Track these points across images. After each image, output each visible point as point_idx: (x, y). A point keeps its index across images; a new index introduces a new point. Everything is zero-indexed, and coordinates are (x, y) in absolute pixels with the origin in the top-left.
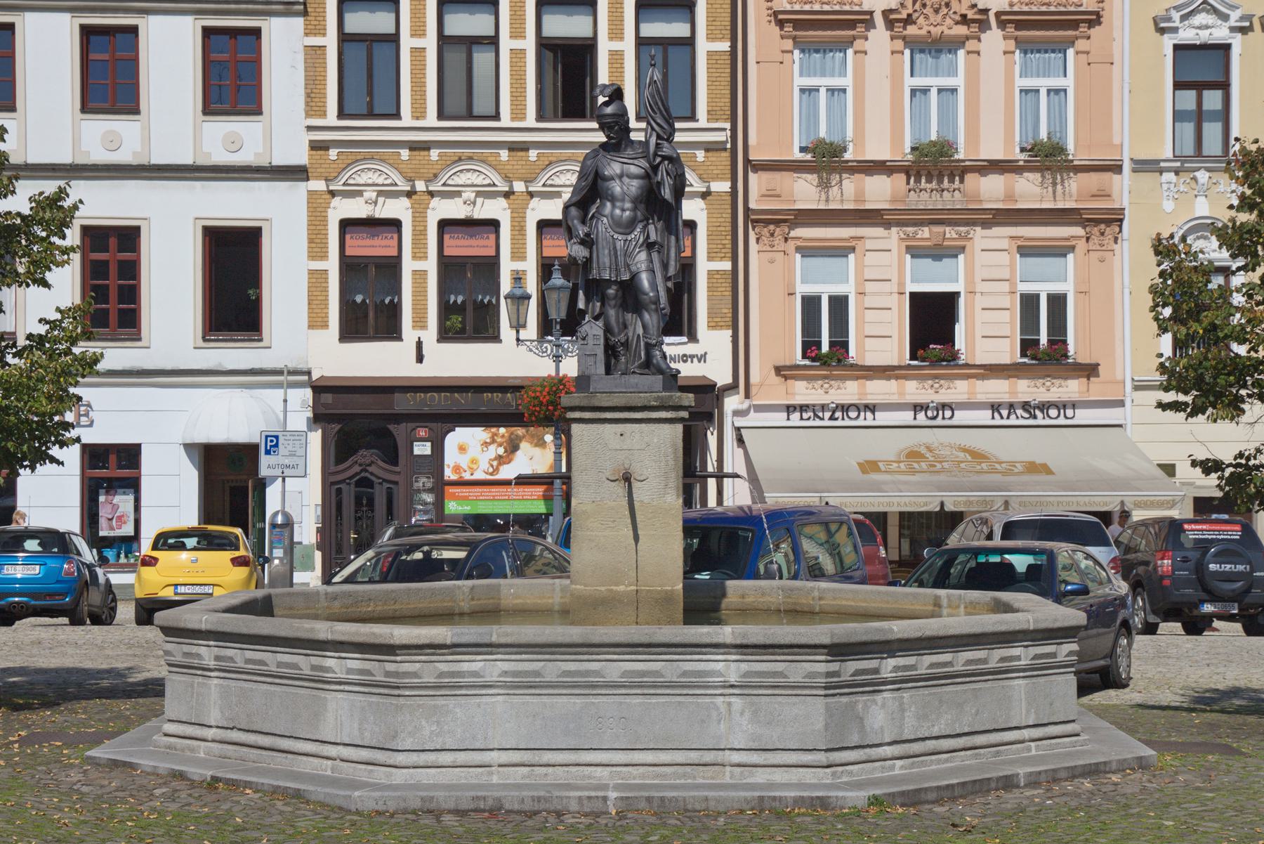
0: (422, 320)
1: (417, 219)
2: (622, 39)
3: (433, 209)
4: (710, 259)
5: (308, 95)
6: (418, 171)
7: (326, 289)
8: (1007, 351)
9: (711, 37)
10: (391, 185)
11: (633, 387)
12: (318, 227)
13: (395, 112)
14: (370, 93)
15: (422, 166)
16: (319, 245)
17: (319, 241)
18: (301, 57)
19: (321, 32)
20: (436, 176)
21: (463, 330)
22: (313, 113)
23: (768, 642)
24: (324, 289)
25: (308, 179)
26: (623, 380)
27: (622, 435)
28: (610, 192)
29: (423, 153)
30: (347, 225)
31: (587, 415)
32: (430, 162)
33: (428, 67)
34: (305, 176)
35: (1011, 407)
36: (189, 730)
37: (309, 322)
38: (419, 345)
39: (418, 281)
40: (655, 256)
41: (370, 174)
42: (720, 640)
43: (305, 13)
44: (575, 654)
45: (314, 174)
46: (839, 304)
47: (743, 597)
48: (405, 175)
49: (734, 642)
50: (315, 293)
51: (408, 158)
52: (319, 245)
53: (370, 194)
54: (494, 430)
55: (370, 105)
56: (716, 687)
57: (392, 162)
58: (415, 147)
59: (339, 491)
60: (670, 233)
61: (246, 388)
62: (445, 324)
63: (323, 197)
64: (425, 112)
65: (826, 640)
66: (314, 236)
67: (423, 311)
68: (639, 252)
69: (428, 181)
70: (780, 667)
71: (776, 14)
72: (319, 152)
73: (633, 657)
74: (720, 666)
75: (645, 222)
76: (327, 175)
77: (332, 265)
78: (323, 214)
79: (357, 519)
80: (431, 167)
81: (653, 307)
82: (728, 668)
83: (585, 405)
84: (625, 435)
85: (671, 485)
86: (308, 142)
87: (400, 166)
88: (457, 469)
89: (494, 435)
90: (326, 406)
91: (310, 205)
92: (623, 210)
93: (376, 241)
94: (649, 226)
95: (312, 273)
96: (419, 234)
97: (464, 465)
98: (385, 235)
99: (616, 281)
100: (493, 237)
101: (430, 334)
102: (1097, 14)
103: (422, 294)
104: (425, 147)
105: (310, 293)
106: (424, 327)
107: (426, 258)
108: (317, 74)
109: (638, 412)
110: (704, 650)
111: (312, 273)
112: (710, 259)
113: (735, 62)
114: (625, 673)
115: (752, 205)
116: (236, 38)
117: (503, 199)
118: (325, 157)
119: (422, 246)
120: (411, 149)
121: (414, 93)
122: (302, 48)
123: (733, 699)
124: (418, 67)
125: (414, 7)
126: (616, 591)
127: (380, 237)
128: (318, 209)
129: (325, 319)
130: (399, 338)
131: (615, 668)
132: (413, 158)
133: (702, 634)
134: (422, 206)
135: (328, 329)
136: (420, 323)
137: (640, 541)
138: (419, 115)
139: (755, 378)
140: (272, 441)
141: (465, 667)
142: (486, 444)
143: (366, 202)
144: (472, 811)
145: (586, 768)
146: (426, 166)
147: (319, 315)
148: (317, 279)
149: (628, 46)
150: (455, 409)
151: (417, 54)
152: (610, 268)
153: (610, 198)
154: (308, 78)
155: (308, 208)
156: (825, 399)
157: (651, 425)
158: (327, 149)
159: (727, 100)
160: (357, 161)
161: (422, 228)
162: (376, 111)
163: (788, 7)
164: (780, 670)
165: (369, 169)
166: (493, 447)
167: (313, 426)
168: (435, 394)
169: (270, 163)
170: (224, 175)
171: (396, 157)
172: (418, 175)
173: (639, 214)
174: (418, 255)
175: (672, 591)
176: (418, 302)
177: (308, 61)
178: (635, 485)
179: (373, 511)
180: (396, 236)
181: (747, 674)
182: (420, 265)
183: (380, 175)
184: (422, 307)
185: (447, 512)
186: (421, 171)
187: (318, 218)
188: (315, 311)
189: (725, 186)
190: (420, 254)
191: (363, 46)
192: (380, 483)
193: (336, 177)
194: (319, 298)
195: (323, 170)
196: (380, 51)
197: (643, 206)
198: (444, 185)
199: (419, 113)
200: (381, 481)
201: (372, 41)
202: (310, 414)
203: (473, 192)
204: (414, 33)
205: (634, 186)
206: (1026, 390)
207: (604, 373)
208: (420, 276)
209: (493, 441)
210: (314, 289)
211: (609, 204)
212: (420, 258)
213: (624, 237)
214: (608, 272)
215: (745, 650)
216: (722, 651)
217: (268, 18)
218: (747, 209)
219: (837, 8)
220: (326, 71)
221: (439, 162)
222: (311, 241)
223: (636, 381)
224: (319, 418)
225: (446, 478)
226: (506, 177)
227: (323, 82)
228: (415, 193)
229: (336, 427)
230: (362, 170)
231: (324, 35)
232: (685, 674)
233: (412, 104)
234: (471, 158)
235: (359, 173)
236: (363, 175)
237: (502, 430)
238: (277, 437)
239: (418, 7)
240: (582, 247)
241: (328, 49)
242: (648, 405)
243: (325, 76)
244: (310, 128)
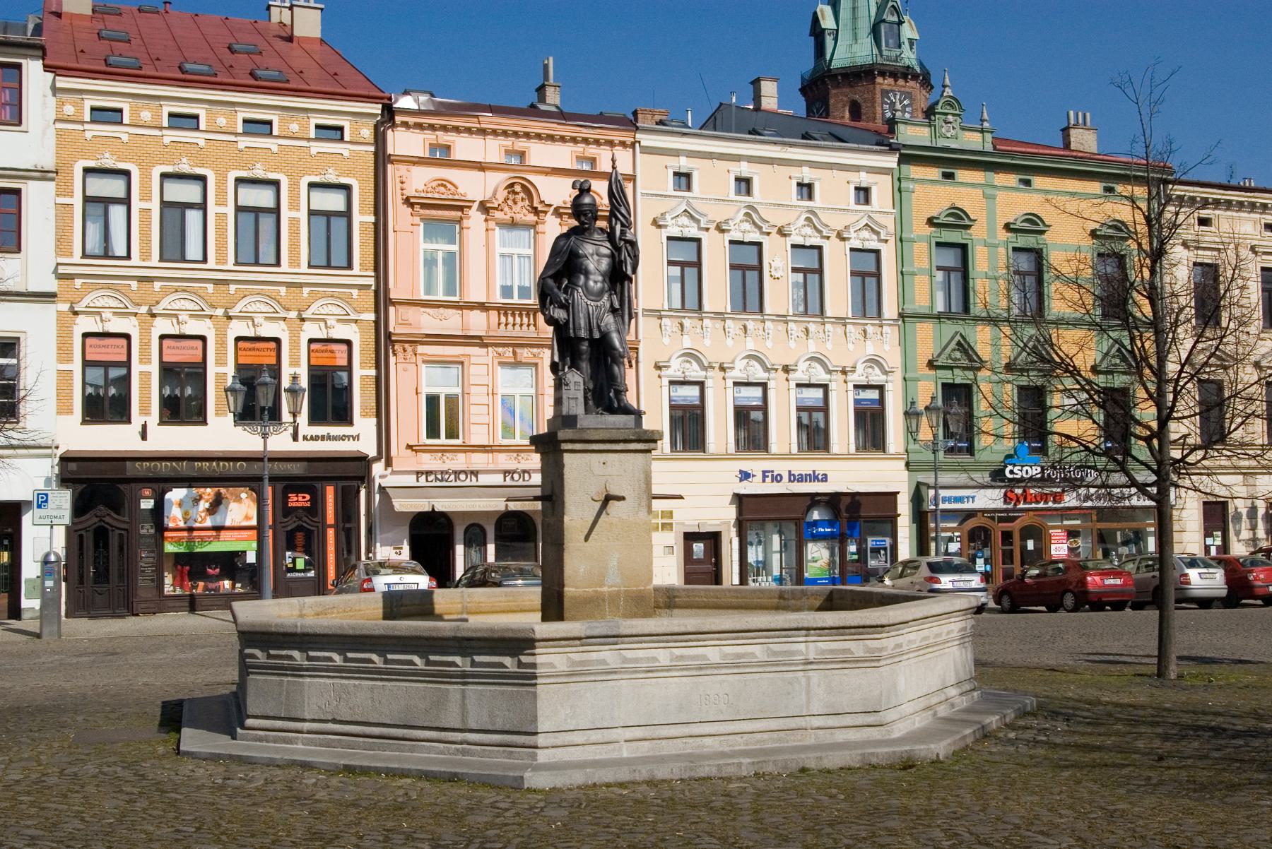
2: (298, 210)
7: (71, 385)
20: (158, 303)
31: (578, 446)
36: (279, 724)
38: (144, 427)
44: (686, 641)
59: (81, 536)
77: (77, 366)
79: (96, 558)
90: (71, 472)
96: (145, 345)
104: (150, 280)
130: (129, 422)
131: (713, 653)
136: (145, 410)
141: (594, 656)
144: (628, 783)
145: (699, 739)
148: (64, 377)
149: (303, 215)
163: (417, 195)
190: (145, 359)
205: (605, 264)
208: (145, 375)
211: (582, 277)
218: (389, 335)
219: (450, 197)
222: (59, 349)
224: (65, 480)
229: (80, 487)
237: (209, 490)
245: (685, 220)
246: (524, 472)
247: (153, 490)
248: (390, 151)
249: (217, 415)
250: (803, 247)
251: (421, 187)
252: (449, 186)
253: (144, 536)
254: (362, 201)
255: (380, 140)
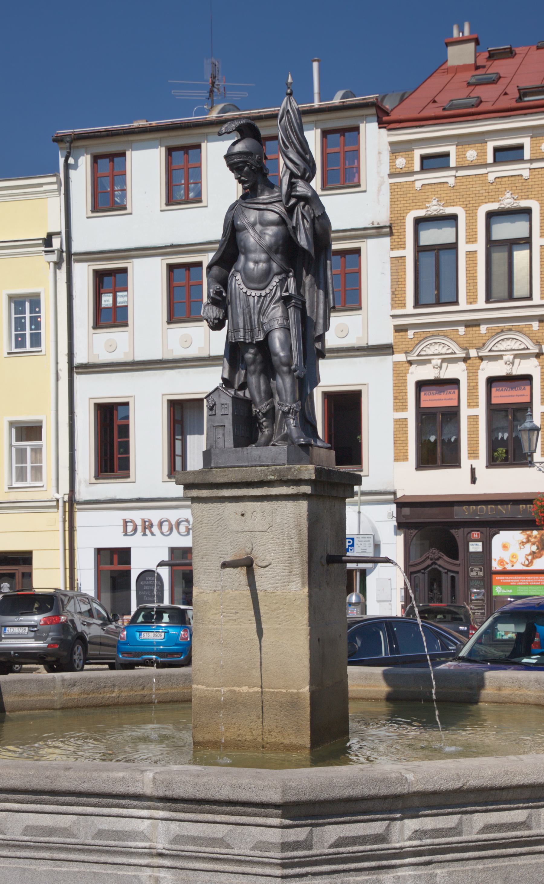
0: (475, 452)
1: (471, 378)
3: (483, 369)
5: (393, 293)
6: (471, 342)
7: (406, 433)
10: (452, 353)
11: (256, 460)
12: (401, 388)
13: (455, 300)
14: (438, 288)
15: (474, 338)
16: (401, 401)
17: (401, 398)
18: (388, 266)
19: (403, 246)
20: (484, 344)
21: (506, 459)
22: (397, 305)
23: (200, 795)
24: (405, 432)
25: (393, 353)
26: (245, 453)
27: (243, 515)
28: (242, 244)
29: (475, 329)
30: (421, 385)
32: (480, 335)
33: (479, 265)
34: (391, 351)
37: (395, 456)
38: (473, 470)
39: (472, 423)
40: (291, 312)
41: (437, 347)
42: (138, 790)
43: (391, 234)
45: (398, 350)
47: (499, 689)
48: (462, 345)
49: (155, 793)
50: (399, 436)
51: (464, 333)
52: (401, 401)
53: (436, 361)
54: (529, 532)
55: (438, 296)
56: (141, 855)
57: (452, 336)
58: (469, 324)
60: (319, 288)
61: (352, 505)
62: (493, 454)
63: (404, 365)
64: (477, 298)
65: (276, 797)
66: (398, 395)
67: (475, 445)
68: (274, 308)
69: (478, 349)
70: (220, 831)
72: (401, 334)
73: (38, 807)
74: (143, 826)
75: (283, 275)
76: (407, 349)
78: (404, 378)
80: (481, 338)
81: (285, 369)
82: (156, 827)
83: (200, 482)
84: (246, 515)
85: (295, 571)
86: (392, 327)
87: (459, 339)
88: (501, 562)
89: (529, 536)
90: (404, 516)
91: (395, 372)
92: (256, 262)
93: (443, 396)
94: (289, 280)
95: (396, 421)
97: (507, 559)
98: (448, 391)
99: (251, 343)
100: (528, 388)
103: (475, 433)
104: (476, 324)
105: (395, 436)
106: (476, 457)
107: (477, 406)
108: (399, 277)
109: (257, 488)
110: (122, 801)
111: (396, 421)
114: (28, 830)
116: (345, 257)
117: (535, 359)
118: (405, 337)
119: (475, 397)
120: (467, 326)
121: (468, 285)
122: (389, 259)
123: (163, 874)
124: (471, 265)
125: (468, 221)
126: (239, 692)
127: (446, 393)
128: (401, 375)
129: (406, 454)
132: (468, 332)
133: (115, 781)
134: (475, 368)
135: (408, 461)
136: (473, 454)
137: (264, 636)
138: (472, 300)
140: (349, 542)
142: (523, 543)
143: (434, 368)
146: (477, 338)
147: (402, 451)
148: (401, 424)
150: (498, 518)
151: (471, 256)
152: (244, 329)
153: (243, 250)
154: (393, 280)
155: (393, 374)
157: (273, 502)
158: (406, 330)
160: (426, 338)
161: (474, 384)
162: (443, 300)
164: (220, 835)
165: (435, 343)
166: (528, 546)
167: (398, 531)
168: (483, 506)
169: (367, 344)
170: (336, 354)
171: (455, 333)
172: (471, 345)
173: (275, 266)
174: (472, 404)
175: (298, 694)
176: (472, 439)
177: (393, 268)
178: (258, 572)
179: (441, 594)
180: (456, 391)
181: (178, 839)
182: (473, 412)
183: (443, 347)
184: (475, 442)
185: (494, 594)
186: (474, 342)
187: (401, 381)
188: (399, 448)
190: (473, 403)
191: (433, 254)
192: (446, 573)
193: (412, 351)
194: (402, 439)
195: (403, 346)
196: (445, 256)
197: (279, 256)
198: (490, 351)
199: (472, 299)
200: (446, 571)
201: (439, 250)
202: (395, 523)
203: (511, 355)
204: (468, 240)
207: (233, 446)
208: (473, 419)
209: (528, 541)
210: (398, 433)
212: (473, 406)
213: (258, 293)
214: (242, 333)
215: (174, 805)
216: (145, 804)
217: (365, 240)
220: (405, 275)
221: (487, 335)
222: (395, 398)
223: (259, 453)
225: (493, 569)
226: (537, 342)
227: (403, 283)
228: (469, 358)
230: (431, 344)
231: (404, 248)
232: (100, 834)
233: (467, 293)
234: (510, 330)
235: (428, 346)
236: (431, 347)
237: (535, 533)
238: (353, 539)
239: (471, 221)
240: (215, 308)
241: (407, 258)
242: (265, 479)
243: (405, 278)
244: (394, 316)
247: (481, 533)
253: (474, 579)
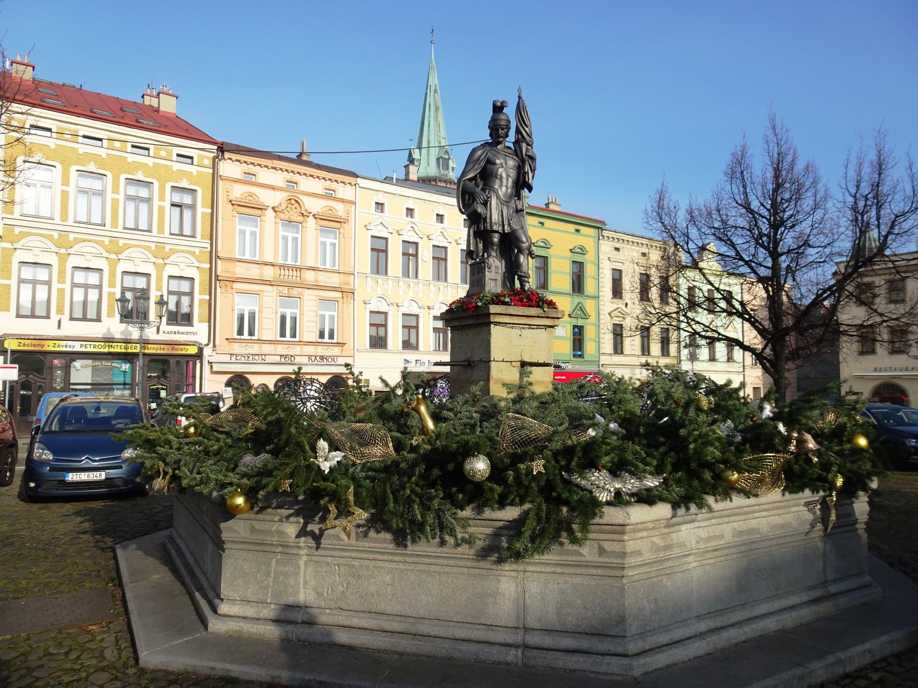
2: (164, 201)
4: (200, 294)
7: (9, 293)
8: (314, 337)
9: (203, 206)
35: (316, 357)
38: (59, 322)
46: (252, 316)
71: (230, 201)
101: (65, 318)
102: (347, 220)
112: (200, 294)
113: (213, 218)
115: (218, 273)
136: (60, 311)
139: (217, 343)
156: (247, 352)
159: (209, 232)
189: (208, 266)
206: (321, 351)
212: (62, 283)
218: (217, 276)
245: (381, 227)
246: (292, 356)
248: (221, 173)
249: (108, 316)
250: (438, 247)
251: (238, 196)
252: (254, 197)
254: (204, 200)
255: (214, 167)
